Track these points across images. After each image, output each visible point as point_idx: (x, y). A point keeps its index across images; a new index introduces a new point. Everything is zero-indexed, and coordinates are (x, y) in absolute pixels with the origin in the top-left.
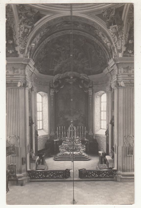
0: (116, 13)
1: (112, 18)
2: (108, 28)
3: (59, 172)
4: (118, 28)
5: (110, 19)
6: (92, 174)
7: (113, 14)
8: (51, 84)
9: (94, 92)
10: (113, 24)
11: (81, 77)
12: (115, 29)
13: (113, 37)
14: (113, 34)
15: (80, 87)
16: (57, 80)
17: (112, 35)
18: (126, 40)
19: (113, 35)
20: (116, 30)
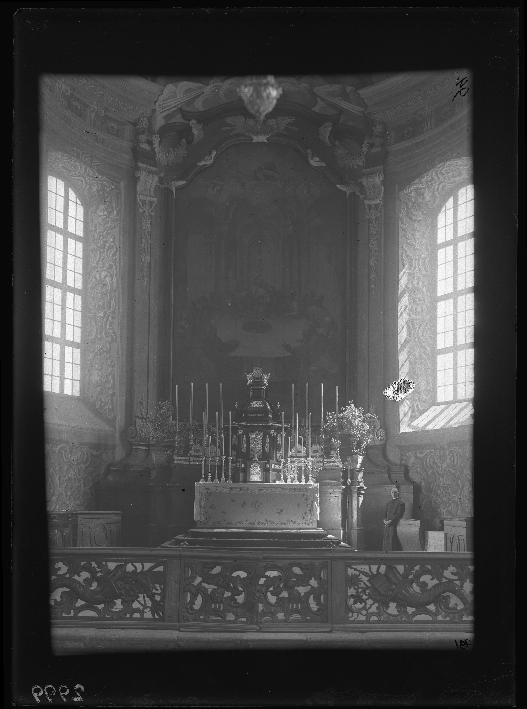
3: (130, 568)
6: (450, 586)
8: (143, 138)
9: (394, 185)
11: (321, 103)
15: (315, 162)
16: (178, 119)
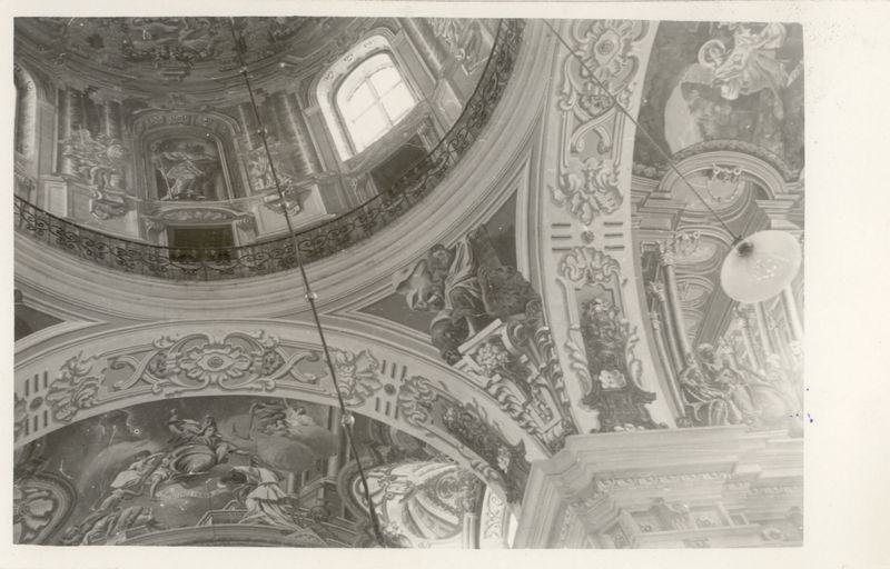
0: (476, 260)
1: (462, 299)
2: (451, 356)
4: (510, 333)
5: (449, 306)
7: (465, 270)
10: (474, 325)
12: (495, 350)
13: (496, 397)
14: (491, 376)
17: (484, 384)
18: (581, 373)
19: (490, 384)
20: (503, 348)
